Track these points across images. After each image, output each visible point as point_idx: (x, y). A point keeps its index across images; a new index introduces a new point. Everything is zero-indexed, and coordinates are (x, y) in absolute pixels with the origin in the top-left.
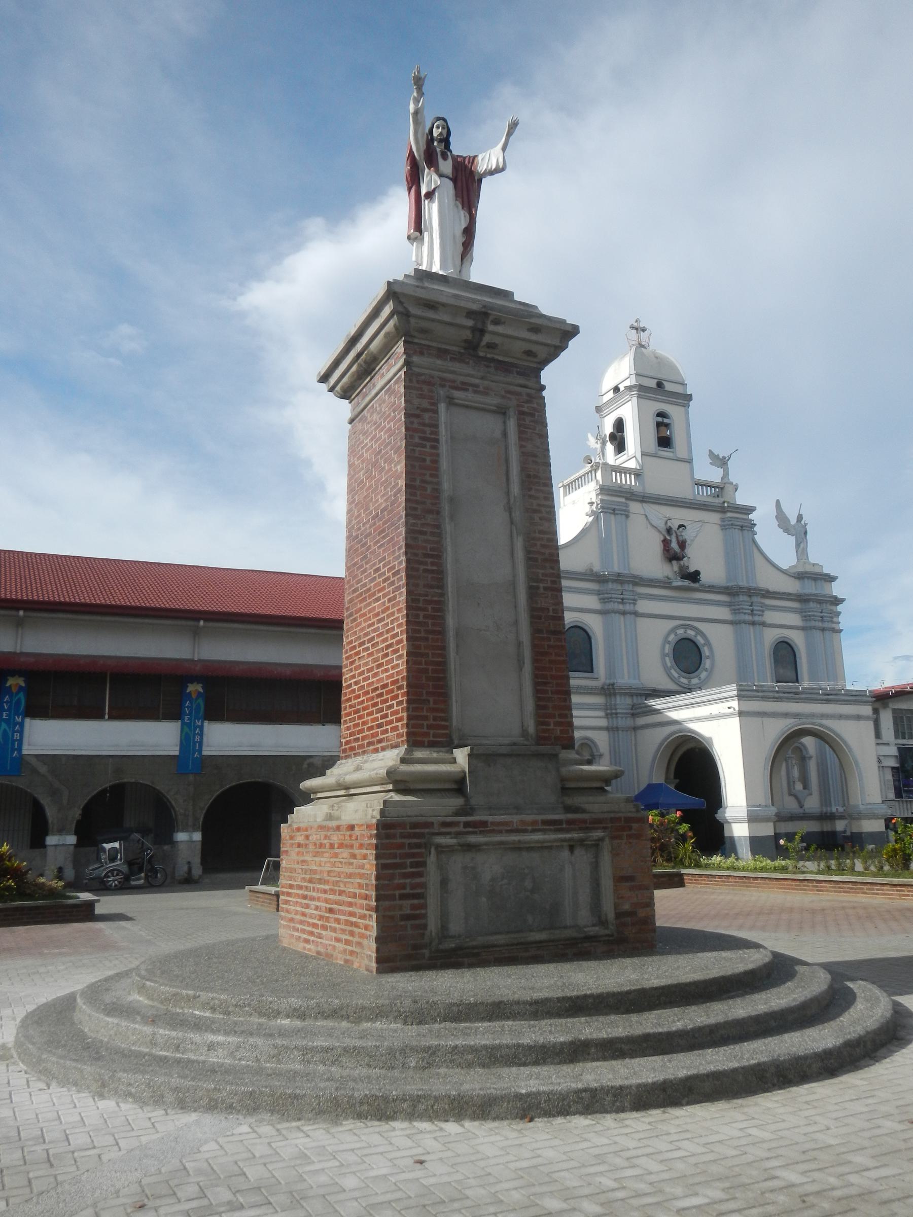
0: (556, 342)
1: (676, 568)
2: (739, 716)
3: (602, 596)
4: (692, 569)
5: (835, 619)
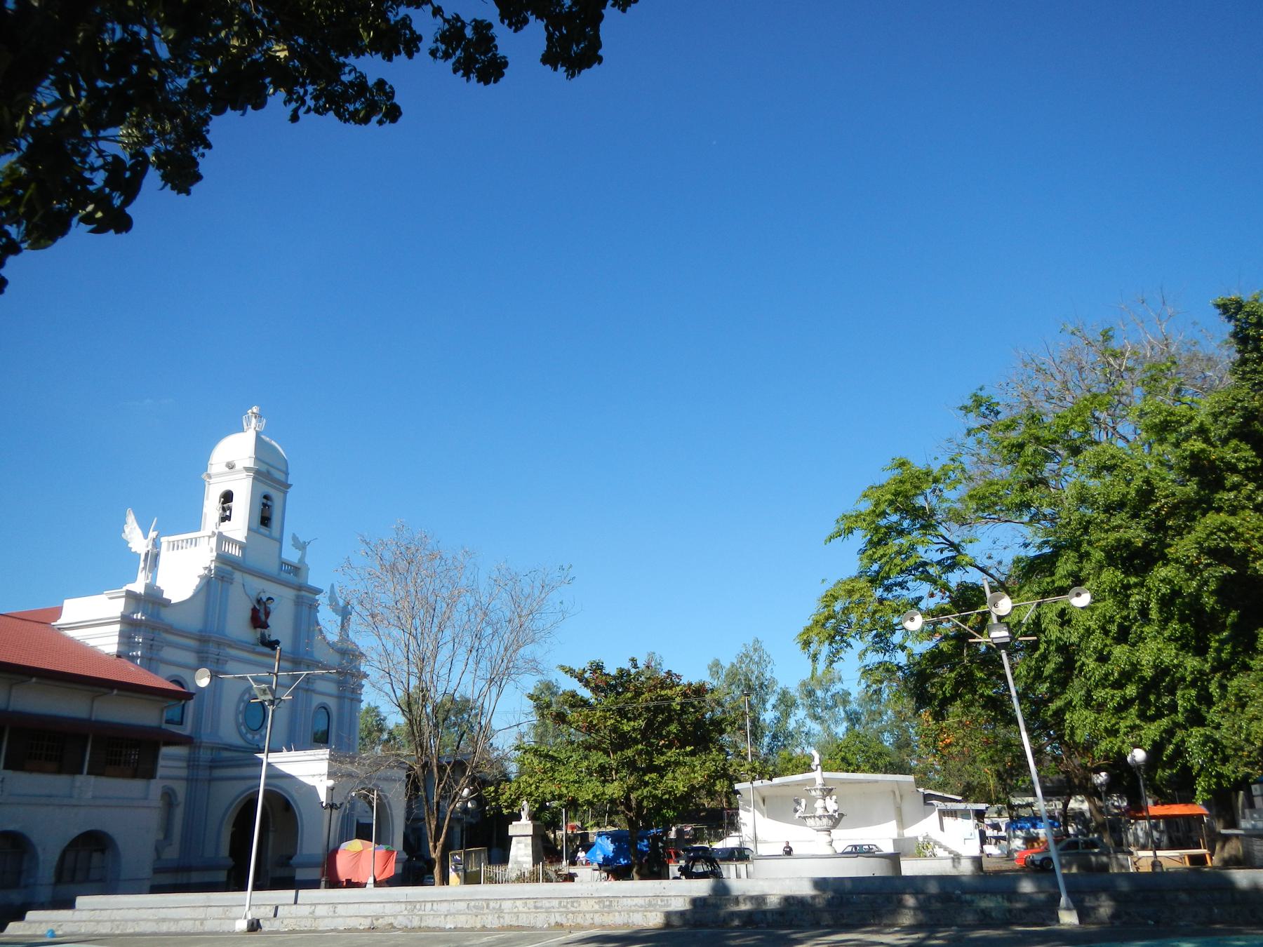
1: (259, 636)
3: (201, 655)
4: (273, 638)
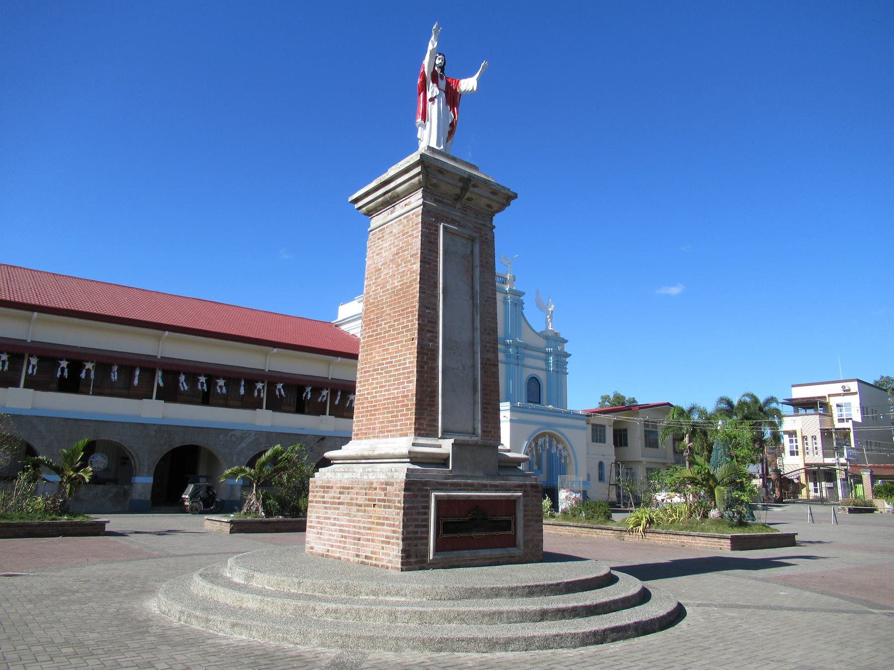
0: (504, 201)
2: (510, 422)
5: (564, 366)
